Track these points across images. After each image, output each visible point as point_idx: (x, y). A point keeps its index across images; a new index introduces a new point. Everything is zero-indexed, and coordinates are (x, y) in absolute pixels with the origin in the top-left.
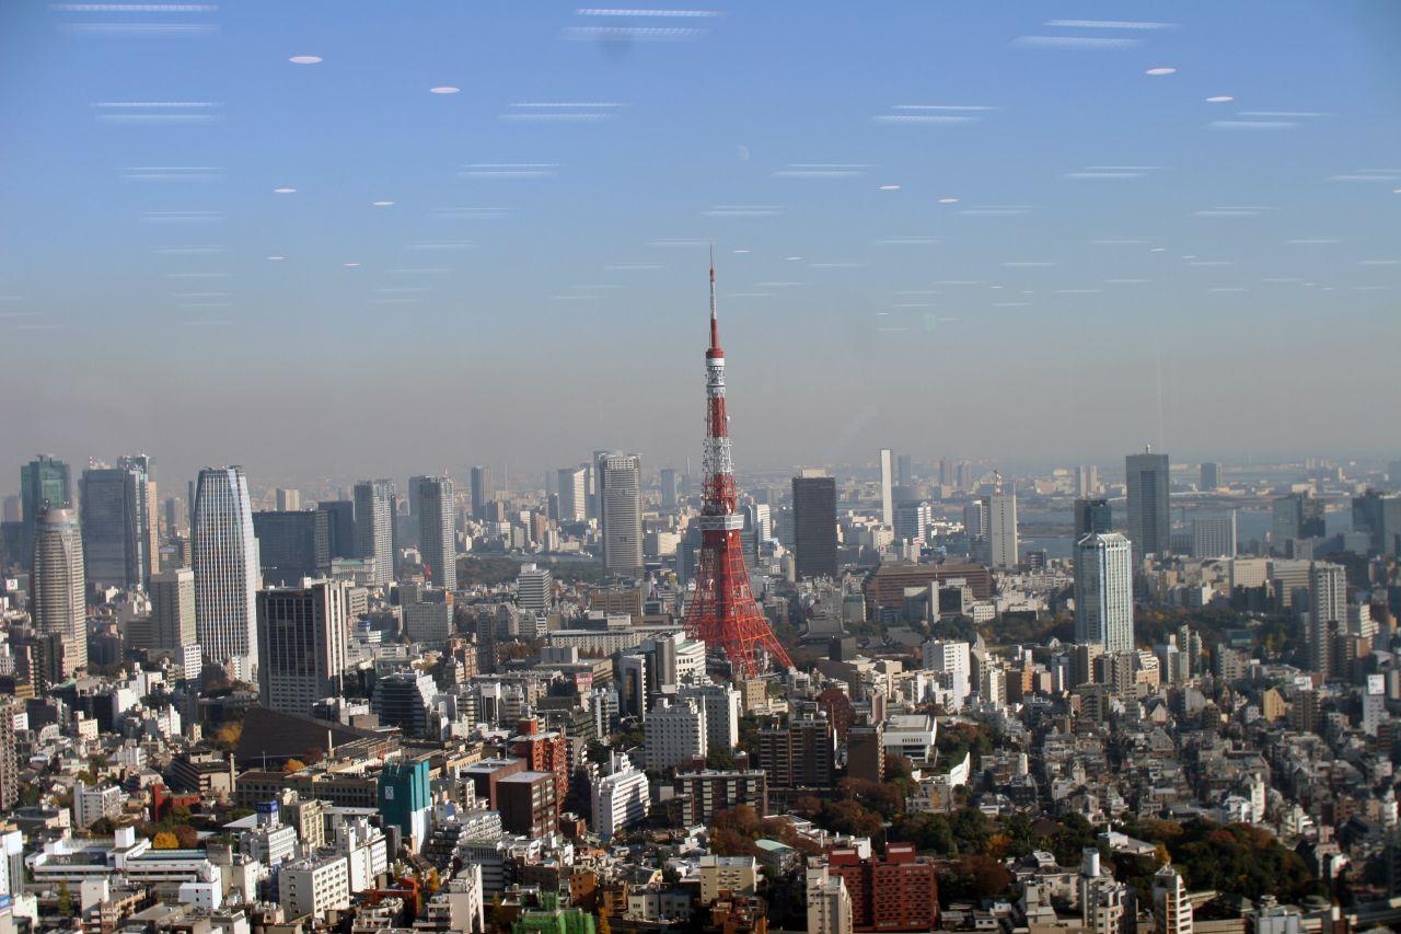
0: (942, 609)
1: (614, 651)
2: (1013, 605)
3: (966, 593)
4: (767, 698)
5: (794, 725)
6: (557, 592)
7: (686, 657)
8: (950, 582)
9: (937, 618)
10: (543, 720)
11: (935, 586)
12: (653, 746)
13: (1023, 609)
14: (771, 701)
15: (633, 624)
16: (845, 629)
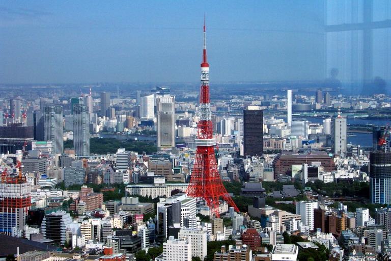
0: (309, 176)
1: (157, 197)
2: (341, 176)
3: (321, 169)
4: (223, 227)
5: (231, 251)
6: (135, 161)
7: (186, 208)
8: (313, 163)
9: (306, 181)
10: (118, 243)
11: (306, 166)
12: (167, 250)
13: (347, 177)
14: (225, 228)
15: (166, 183)
16: (263, 187)
